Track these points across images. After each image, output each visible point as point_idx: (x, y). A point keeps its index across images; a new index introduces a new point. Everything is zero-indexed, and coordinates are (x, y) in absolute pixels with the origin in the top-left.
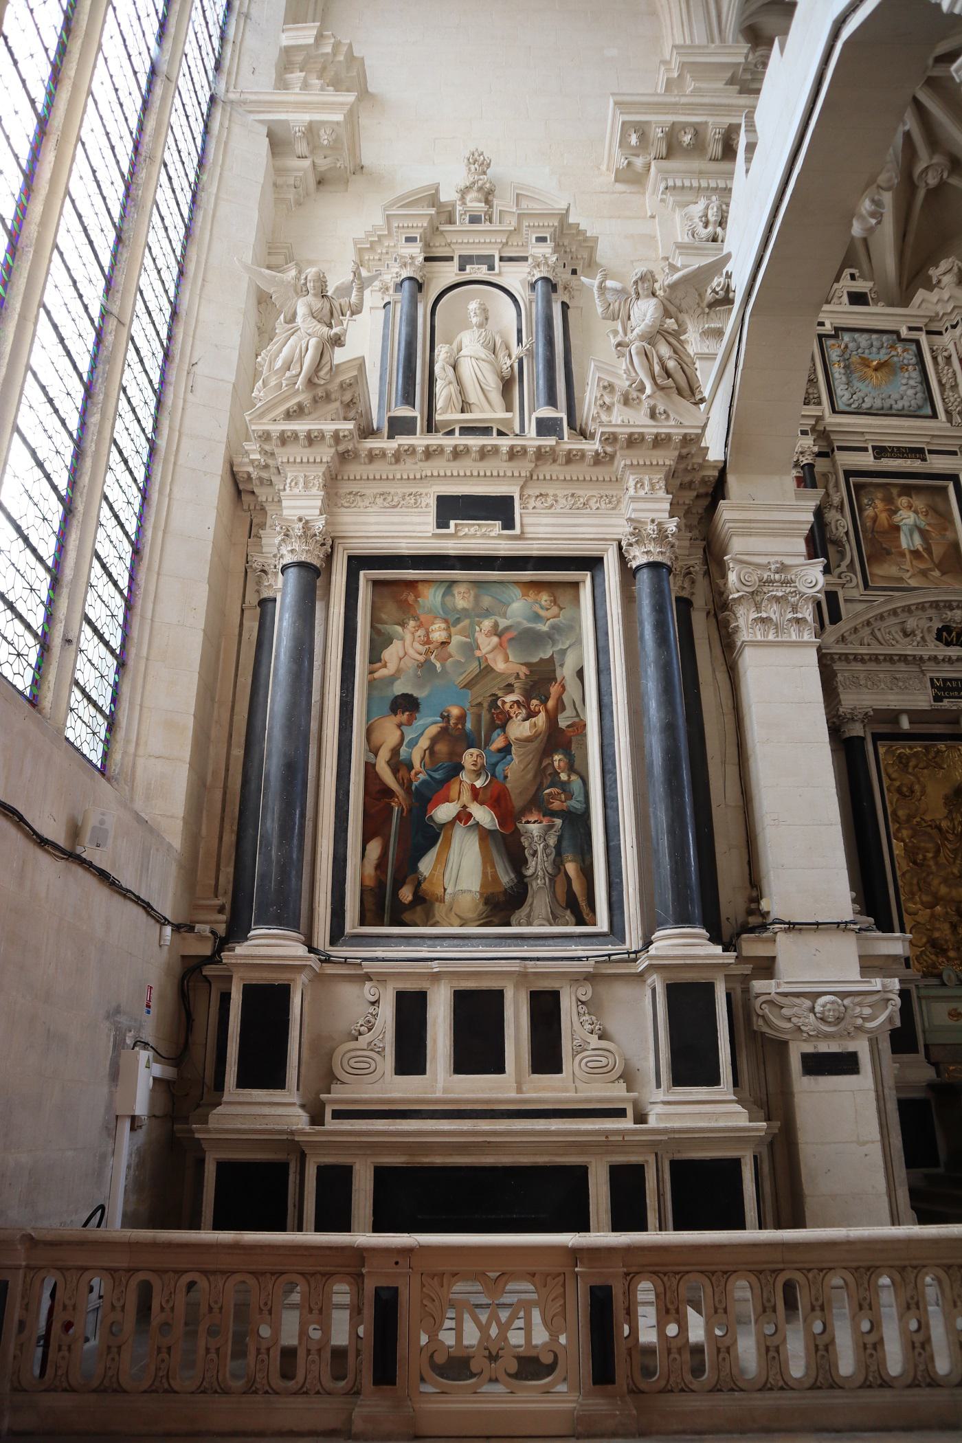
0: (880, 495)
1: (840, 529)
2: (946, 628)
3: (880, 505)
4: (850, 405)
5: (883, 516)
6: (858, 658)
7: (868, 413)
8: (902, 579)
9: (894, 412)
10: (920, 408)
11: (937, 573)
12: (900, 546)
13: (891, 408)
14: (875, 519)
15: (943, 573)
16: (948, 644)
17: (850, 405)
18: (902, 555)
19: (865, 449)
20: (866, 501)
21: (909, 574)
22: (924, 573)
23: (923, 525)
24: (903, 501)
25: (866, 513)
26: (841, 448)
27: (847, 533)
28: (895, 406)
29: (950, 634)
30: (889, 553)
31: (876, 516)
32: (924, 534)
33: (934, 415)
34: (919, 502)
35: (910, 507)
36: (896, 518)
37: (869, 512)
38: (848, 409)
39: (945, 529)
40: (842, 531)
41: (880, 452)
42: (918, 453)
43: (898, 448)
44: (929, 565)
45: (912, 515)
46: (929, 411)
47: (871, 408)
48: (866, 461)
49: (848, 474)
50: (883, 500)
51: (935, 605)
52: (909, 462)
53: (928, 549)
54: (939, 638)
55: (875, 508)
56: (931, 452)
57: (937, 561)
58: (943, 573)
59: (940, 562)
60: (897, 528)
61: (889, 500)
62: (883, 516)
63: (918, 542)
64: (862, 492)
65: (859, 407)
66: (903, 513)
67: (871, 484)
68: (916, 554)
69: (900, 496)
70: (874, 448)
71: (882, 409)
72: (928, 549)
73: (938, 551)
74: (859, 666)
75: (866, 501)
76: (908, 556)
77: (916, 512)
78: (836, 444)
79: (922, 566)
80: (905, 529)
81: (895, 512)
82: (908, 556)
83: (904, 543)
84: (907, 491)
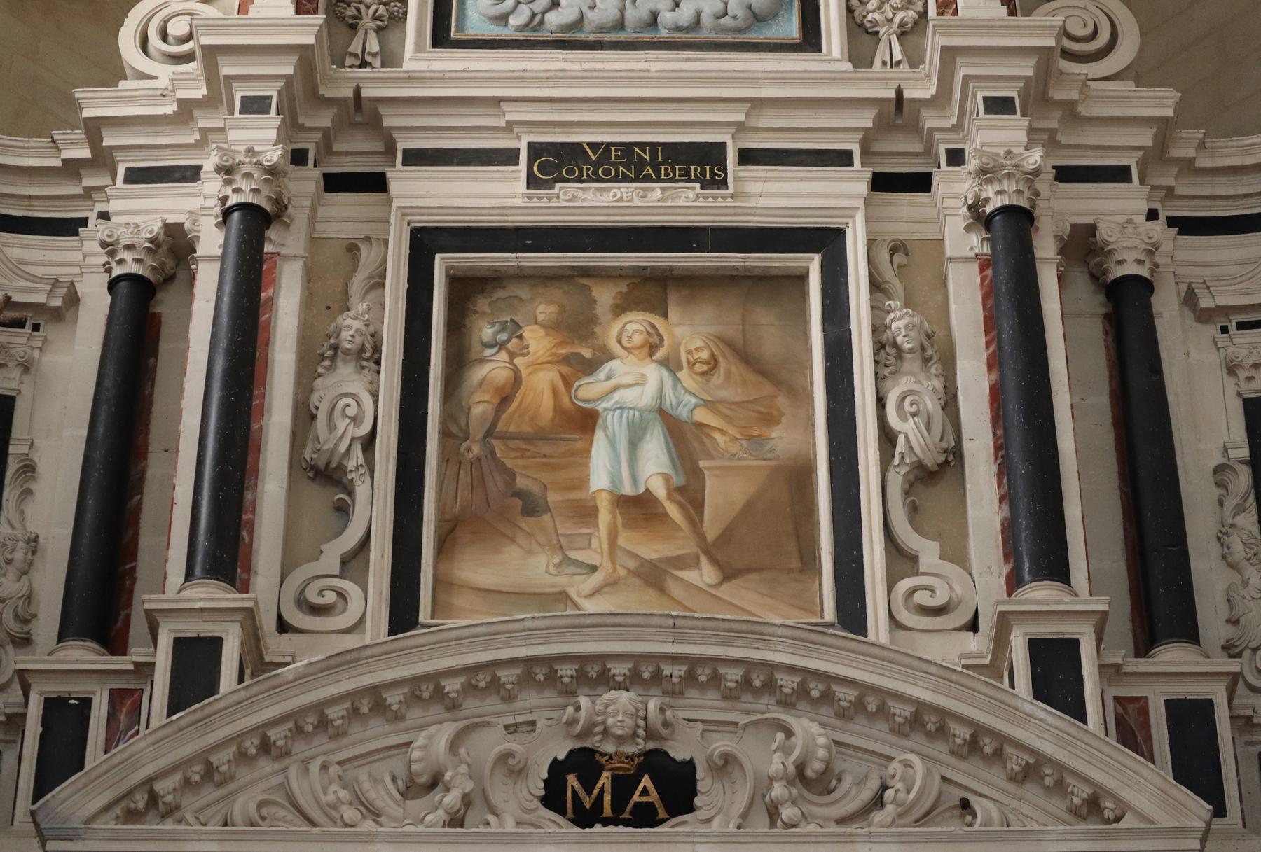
0: (545, 311)
1: (342, 425)
2: (583, 762)
3: (537, 341)
4: (503, 19)
5: (541, 384)
7: (570, 41)
8: (563, 597)
9: (663, 34)
10: (758, 18)
11: (706, 574)
12: (583, 483)
13: (654, 16)
14: (505, 398)
15: (729, 574)
16: (585, 818)
17: (503, 19)
18: (585, 513)
19: (509, 157)
20: (487, 332)
21: (596, 579)
22: (653, 576)
23: (686, 405)
24: (635, 324)
25: (478, 374)
26: (416, 158)
27: (369, 442)
28: (666, 17)
29: (589, 782)
30: (532, 507)
31: (517, 380)
32: (683, 438)
33: (811, 39)
34: (690, 329)
35: (652, 348)
36: (589, 389)
37: (491, 370)
38: (495, 31)
39: (770, 419)
40: (347, 432)
41: (555, 162)
42: (701, 162)
43: (627, 148)
44: (683, 545)
45: (653, 373)
46: (791, 27)
47: (578, 24)
48: (501, 195)
49: (426, 243)
50: (553, 327)
51: (540, 672)
52: (656, 191)
53: (690, 494)
54: (553, 798)
55: (518, 356)
56: (747, 157)
57: (712, 530)
58: (729, 574)
59: (727, 535)
60: (586, 421)
61: (578, 326)
62: (541, 384)
63: (654, 466)
64: (482, 304)
65: (535, 21)
66: (621, 369)
67: (522, 276)
68: (638, 508)
69: (620, 309)
70: (535, 150)
71: (620, 25)
72: (690, 494)
73: (724, 495)
75: (487, 332)
76: (604, 516)
77: (672, 365)
78: (405, 143)
79: (652, 550)
80: (614, 425)
81: (590, 367)
82: (604, 517)
83: (602, 469)
84: (651, 291)
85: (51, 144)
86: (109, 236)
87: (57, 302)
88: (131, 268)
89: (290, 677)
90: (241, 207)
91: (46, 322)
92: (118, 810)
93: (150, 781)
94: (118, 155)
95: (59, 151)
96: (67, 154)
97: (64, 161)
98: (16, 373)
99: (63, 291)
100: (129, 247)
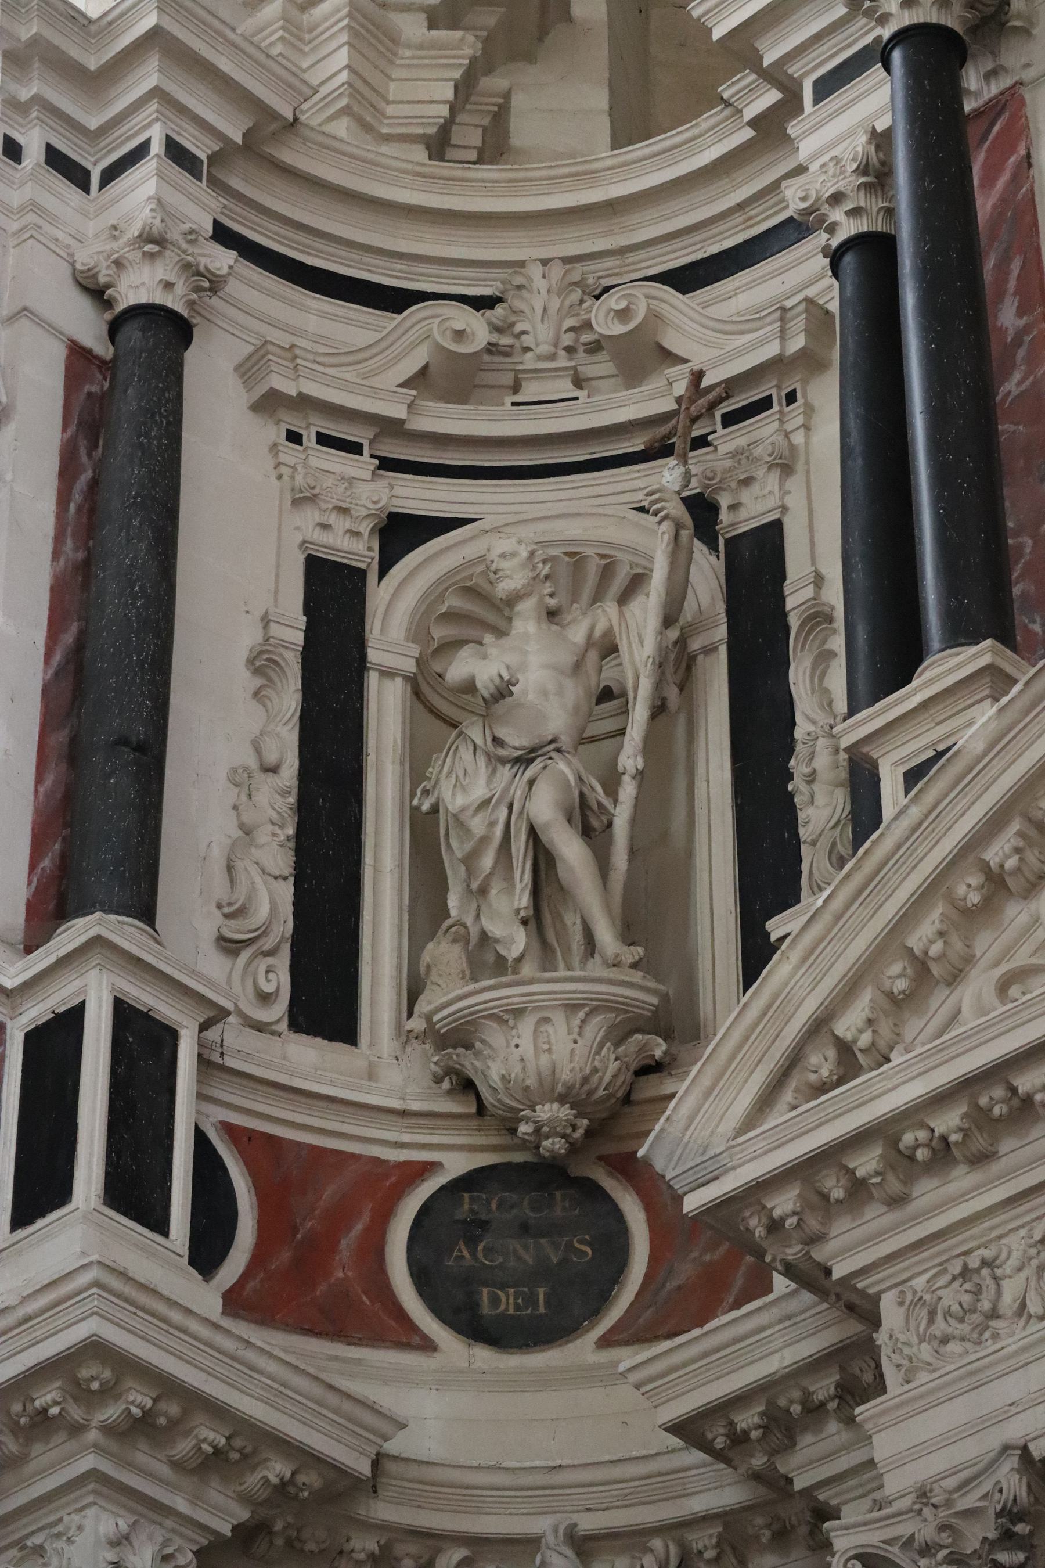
6: (907, 1154)
74: (953, 1198)
85: (728, 112)
86: (803, 199)
87: (797, 343)
88: (849, 229)
89: (980, 746)
90: (900, 37)
91: (805, 382)
92: (788, 1096)
93: (819, 1026)
94: (795, 70)
95: (740, 111)
96: (751, 112)
97: (753, 123)
98: (773, 480)
99: (798, 324)
100: (836, 199)
